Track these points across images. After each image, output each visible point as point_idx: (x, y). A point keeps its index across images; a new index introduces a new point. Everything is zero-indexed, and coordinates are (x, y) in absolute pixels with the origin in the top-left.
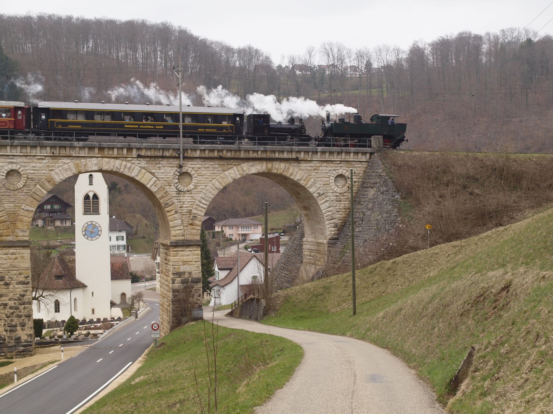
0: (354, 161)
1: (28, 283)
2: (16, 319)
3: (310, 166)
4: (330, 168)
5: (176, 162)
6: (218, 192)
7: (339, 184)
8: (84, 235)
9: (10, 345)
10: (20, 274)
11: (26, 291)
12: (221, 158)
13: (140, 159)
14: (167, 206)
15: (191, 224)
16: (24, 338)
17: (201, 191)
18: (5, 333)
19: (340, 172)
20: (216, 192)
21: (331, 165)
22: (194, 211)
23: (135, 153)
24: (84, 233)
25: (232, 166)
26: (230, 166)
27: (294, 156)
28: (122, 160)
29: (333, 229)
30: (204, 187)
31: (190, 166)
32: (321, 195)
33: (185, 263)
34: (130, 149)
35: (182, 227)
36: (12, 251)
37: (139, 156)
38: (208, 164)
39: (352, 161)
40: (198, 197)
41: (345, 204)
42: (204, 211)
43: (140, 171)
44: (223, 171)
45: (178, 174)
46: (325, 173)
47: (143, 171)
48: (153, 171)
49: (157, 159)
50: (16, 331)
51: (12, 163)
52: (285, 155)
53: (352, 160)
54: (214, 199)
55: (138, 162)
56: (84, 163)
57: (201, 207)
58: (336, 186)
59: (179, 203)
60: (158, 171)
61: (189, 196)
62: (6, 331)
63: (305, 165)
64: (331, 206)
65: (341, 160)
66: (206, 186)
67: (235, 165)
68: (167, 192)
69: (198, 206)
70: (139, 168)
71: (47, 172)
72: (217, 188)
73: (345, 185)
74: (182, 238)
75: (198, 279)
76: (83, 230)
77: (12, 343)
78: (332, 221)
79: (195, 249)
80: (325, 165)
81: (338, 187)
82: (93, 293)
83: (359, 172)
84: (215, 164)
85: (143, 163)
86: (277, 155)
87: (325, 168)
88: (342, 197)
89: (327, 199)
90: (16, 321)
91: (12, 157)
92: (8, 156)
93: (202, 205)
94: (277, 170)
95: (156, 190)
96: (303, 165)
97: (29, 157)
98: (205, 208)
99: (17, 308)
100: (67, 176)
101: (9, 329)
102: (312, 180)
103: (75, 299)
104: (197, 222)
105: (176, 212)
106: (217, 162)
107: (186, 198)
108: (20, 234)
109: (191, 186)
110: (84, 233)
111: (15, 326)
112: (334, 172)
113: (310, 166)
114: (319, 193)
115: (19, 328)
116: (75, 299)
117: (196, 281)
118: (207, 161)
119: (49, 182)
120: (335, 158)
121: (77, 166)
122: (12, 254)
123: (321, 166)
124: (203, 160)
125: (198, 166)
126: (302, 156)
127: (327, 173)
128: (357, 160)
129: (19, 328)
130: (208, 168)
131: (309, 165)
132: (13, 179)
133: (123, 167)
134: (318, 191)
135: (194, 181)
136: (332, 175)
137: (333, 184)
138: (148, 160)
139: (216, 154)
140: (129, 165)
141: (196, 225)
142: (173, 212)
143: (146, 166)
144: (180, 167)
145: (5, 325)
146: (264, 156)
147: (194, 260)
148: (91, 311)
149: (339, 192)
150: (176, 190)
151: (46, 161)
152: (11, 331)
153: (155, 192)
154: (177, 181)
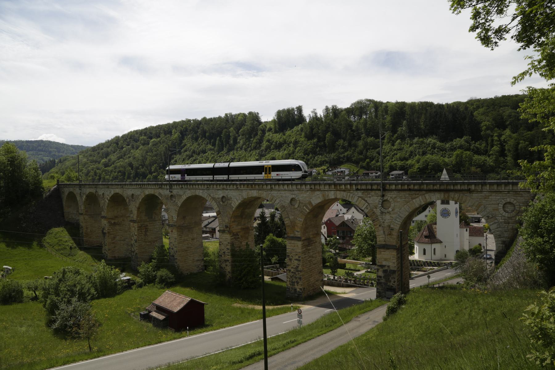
0: (521, 191)
1: (299, 261)
2: (294, 278)
3: (480, 196)
4: (499, 197)
5: (380, 193)
6: (408, 213)
7: (508, 210)
8: (441, 215)
9: (292, 292)
10: (296, 255)
11: (299, 264)
12: (410, 190)
13: (358, 191)
14: (374, 221)
15: (390, 234)
16: (298, 290)
17: (397, 213)
18: (289, 285)
19: (508, 200)
20: (407, 214)
21: (500, 195)
22: (392, 226)
23: (354, 187)
24: (441, 214)
25: (418, 196)
26: (417, 196)
27: (466, 187)
28: (348, 192)
29: (501, 245)
30: (399, 210)
31: (390, 196)
32: (490, 218)
33: (386, 260)
34: (351, 184)
35: (384, 236)
36: (292, 242)
37: (357, 190)
38: (402, 194)
39: (519, 191)
40: (394, 216)
41: (513, 226)
42: (399, 226)
43: (358, 199)
44: (413, 199)
45: (381, 201)
46: (494, 201)
47: (360, 199)
48: (366, 199)
49: (368, 191)
50: (295, 285)
51: (293, 194)
52: (458, 187)
53: (520, 190)
54: (405, 218)
55: (356, 193)
56: (327, 194)
57: (397, 223)
58: (505, 211)
59: (382, 220)
60: (369, 199)
61: (388, 216)
62: (290, 284)
63: (476, 195)
64: (500, 227)
65: (509, 190)
66: (400, 209)
67: (421, 195)
68: (374, 212)
69: (395, 222)
70: (357, 197)
71: (309, 199)
72: (407, 211)
73: (513, 211)
74: (384, 243)
75: (394, 270)
76: (441, 212)
77: (293, 291)
78: (500, 239)
79: (392, 251)
80: (494, 194)
81: (507, 212)
82: (445, 246)
83: (526, 201)
84: (407, 194)
85: (360, 193)
86: (452, 188)
87: (495, 197)
88: (510, 221)
89: (496, 221)
90: (294, 280)
91: (292, 191)
92: (291, 190)
93: (397, 222)
94: (453, 199)
95: (368, 211)
96: (475, 195)
97: (300, 191)
98: (399, 224)
99: (295, 273)
100: (319, 202)
101: (291, 283)
102: (482, 206)
103: (434, 249)
104: (393, 233)
105: (380, 226)
106: (408, 192)
107: (387, 217)
108: (296, 233)
109: (390, 209)
110: (441, 214)
111: (294, 282)
112: (503, 201)
113: (480, 196)
114: (488, 217)
115: (296, 284)
116: (434, 249)
117: (394, 272)
118: (400, 192)
119: (310, 205)
120: (503, 188)
121: (323, 196)
122: (293, 243)
123: (491, 196)
124: (398, 192)
125: (394, 196)
126: (473, 187)
127: (496, 201)
128: (524, 191)
129: (296, 284)
130: (402, 197)
131: (480, 195)
132: (293, 203)
133: (348, 196)
134: (487, 215)
135: (392, 205)
136: (501, 202)
137: (502, 209)
138: (363, 191)
139: (406, 187)
140: (351, 195)
141: (393, 235)
142: (378, 226)
143: (362, 196)
144: (383, 196)
145: (290, 281)
146: (442, 187)
147: (392, 258)
148: (444, 256)
149: (507, 216)
150: (380, 212)
151: (308, 193)
152: (292, 285)
153: (367, 212)
154: (380, 205)
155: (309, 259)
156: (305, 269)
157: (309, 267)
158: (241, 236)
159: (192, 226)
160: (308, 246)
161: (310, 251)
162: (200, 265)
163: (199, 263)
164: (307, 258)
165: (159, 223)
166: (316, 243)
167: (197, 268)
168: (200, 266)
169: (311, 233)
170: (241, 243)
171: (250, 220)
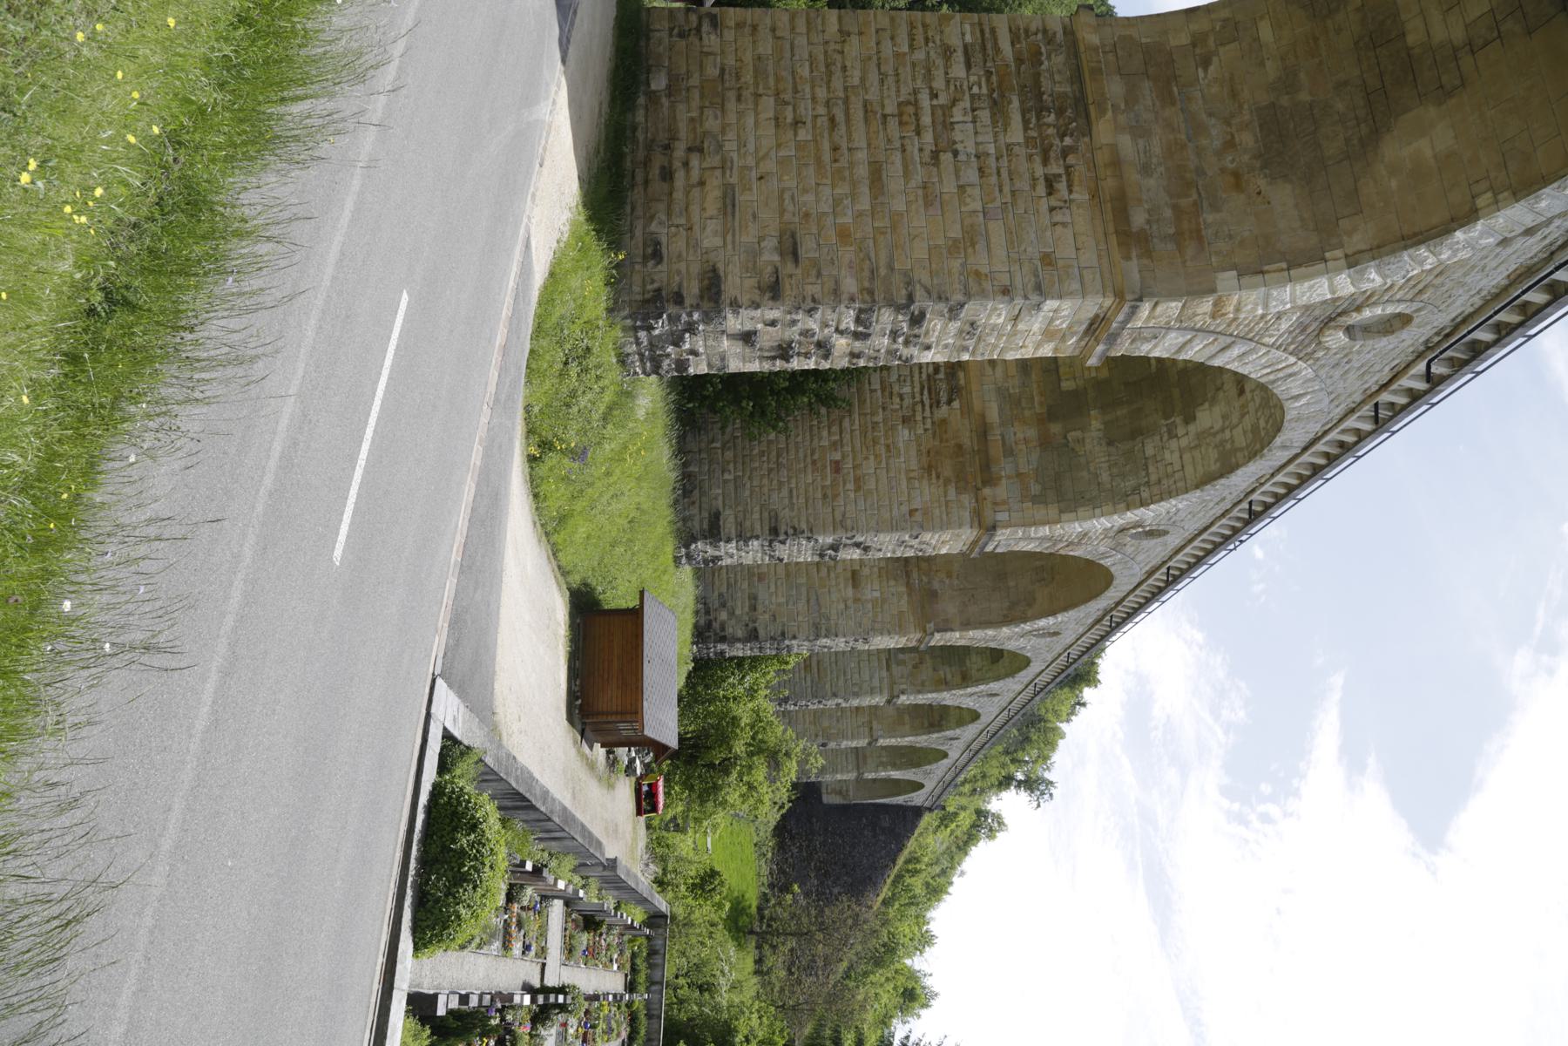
155: (925, 101)
156: (854, 39)
157: (866, 104)
158: (944, 421)
159: (915, 575)
160: (1036, 104)
161: (985, 115)
162: (732, 614)
163: (738, 612)
164: (939, 84)
165: (881, 680)
166: (1044, 205)
167: (721, 595)
168: (724, 616)
169: (1126, 143)
170: (905, 420)
171: (1035, 489)
